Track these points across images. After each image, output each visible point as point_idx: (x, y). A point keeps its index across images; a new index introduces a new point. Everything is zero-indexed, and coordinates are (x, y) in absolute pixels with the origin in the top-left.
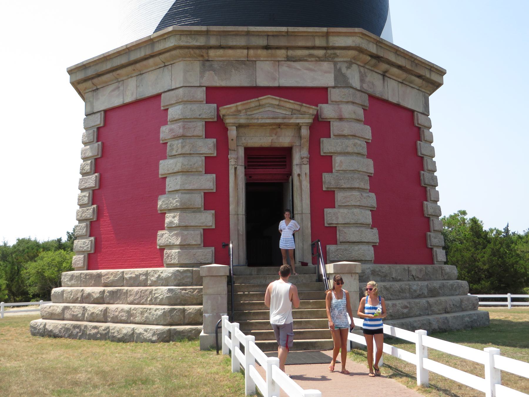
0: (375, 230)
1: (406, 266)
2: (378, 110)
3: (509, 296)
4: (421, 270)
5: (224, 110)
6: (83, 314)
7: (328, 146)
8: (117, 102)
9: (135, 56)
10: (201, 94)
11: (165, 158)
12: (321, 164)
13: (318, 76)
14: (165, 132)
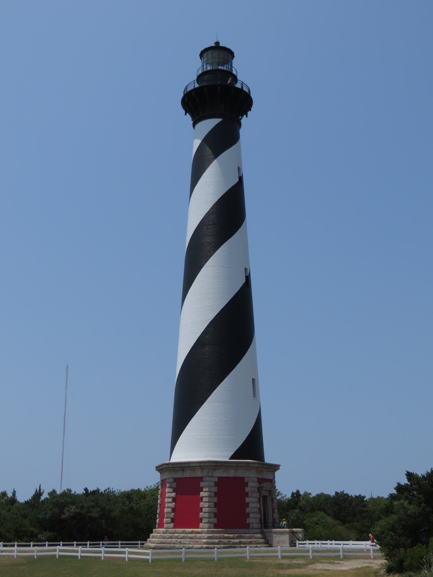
3: (120, 542)
5: (261, 485)
6: (229, 543)
8: (225, 475)
9: (239, 465)
10: (256, 480)
11: (248, 497)
14: (247, 489)
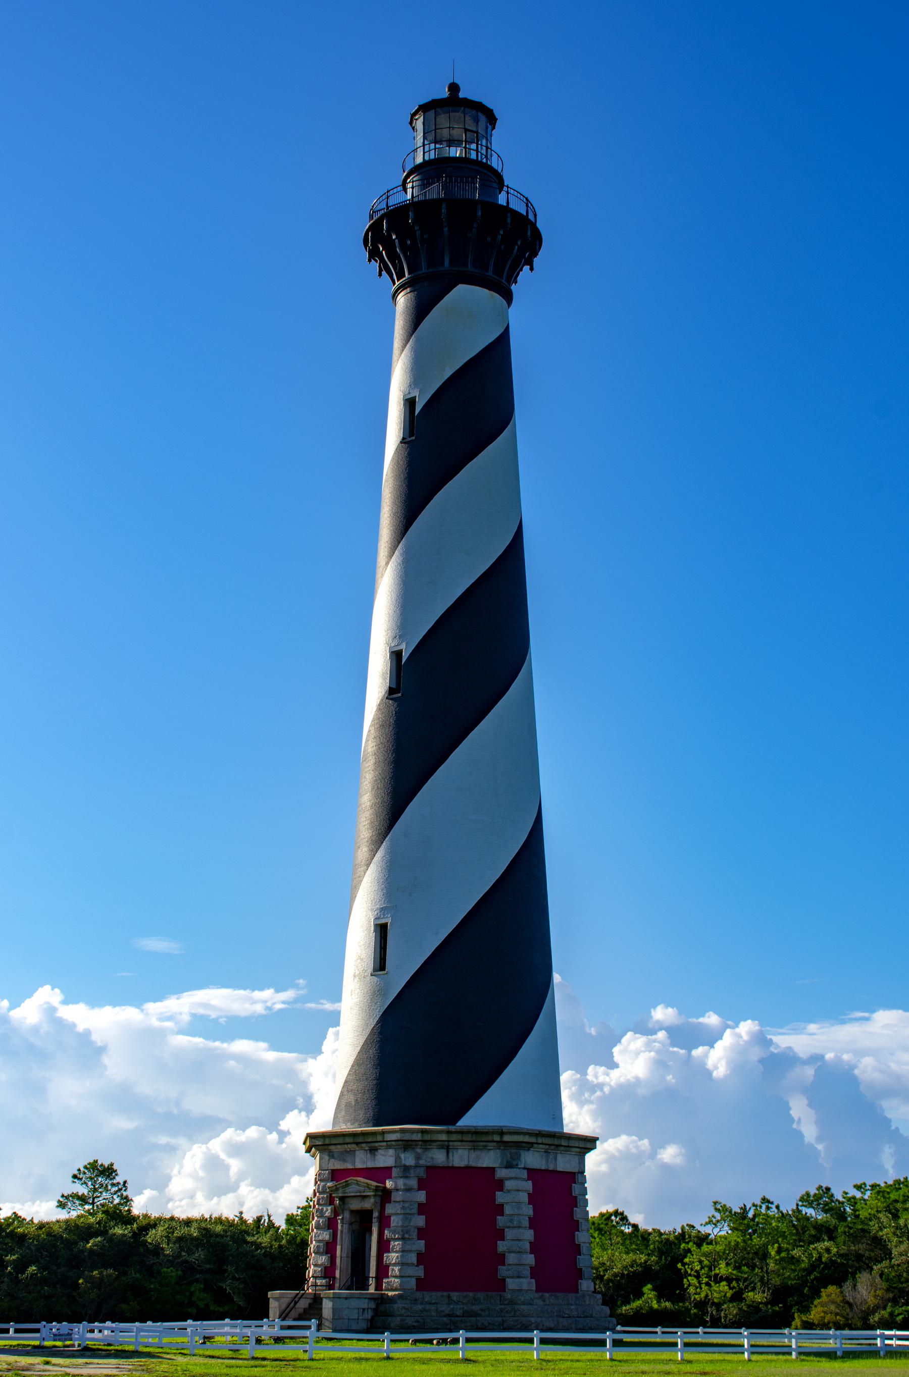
0: (422, 1267)
1: (445, 1294)
2: (434, 1179)
4: (465, 1297)
7: (389, 1209)
12: (384, 1222)
13: (385, 1159)
